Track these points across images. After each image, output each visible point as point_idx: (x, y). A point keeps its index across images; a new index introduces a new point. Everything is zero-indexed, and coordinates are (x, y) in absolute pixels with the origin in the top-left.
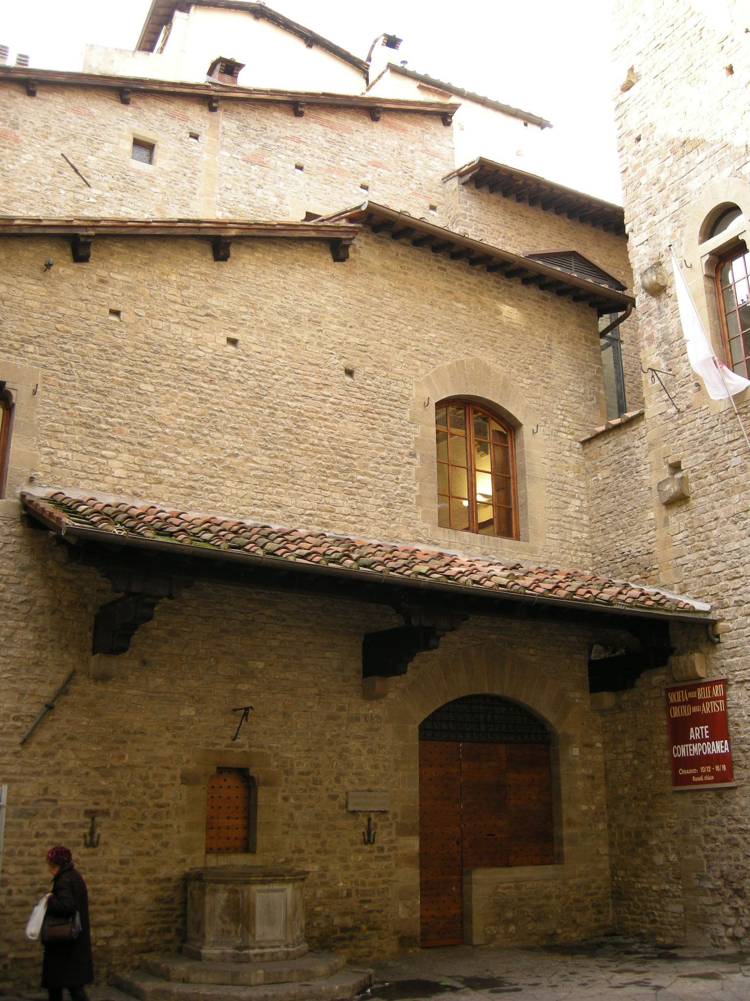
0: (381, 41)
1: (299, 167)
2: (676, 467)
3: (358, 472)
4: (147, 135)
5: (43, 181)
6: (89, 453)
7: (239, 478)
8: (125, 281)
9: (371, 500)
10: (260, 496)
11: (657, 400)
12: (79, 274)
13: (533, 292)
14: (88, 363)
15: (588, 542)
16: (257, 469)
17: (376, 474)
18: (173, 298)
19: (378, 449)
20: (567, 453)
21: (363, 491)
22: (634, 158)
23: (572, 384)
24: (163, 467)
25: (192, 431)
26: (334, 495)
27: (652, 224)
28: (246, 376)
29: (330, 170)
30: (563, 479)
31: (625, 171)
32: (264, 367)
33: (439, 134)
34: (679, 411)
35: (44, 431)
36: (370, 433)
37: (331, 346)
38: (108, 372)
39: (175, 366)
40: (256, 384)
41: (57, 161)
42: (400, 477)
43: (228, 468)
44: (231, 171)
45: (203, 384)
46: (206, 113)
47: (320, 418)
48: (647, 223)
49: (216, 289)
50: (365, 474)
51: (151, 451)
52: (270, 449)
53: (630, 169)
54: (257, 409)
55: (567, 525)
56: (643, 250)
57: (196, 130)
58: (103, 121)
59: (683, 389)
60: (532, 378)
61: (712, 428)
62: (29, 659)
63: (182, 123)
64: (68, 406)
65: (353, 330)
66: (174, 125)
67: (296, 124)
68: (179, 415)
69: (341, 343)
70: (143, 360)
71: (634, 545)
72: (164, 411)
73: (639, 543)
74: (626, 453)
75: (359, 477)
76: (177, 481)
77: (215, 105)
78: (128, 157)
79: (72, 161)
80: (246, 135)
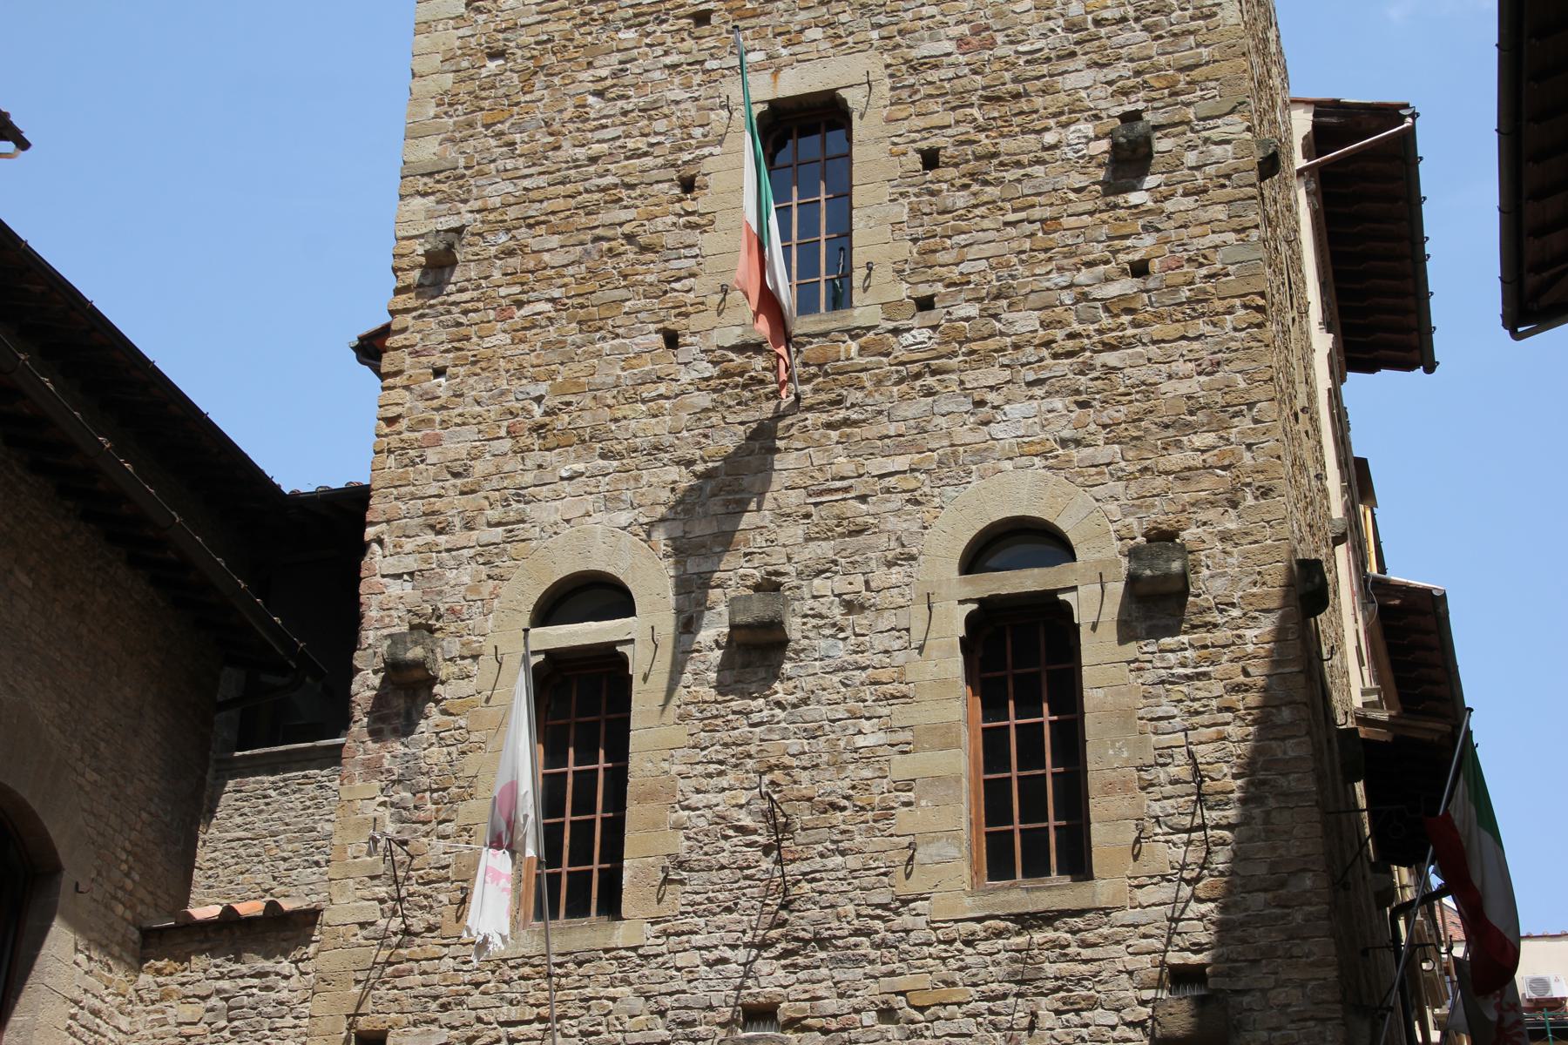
11: (359, 893)
22: (421, 405)
23: (156, 800)
27: (429, 547)
30: (98, 1004)
31: (390, 421)
48: (420, 541)
53: (403, 424)
56: (395, 588)
59: (425, 889)
60: (98, 770)
61: (477, 985)
74: (255, 981)
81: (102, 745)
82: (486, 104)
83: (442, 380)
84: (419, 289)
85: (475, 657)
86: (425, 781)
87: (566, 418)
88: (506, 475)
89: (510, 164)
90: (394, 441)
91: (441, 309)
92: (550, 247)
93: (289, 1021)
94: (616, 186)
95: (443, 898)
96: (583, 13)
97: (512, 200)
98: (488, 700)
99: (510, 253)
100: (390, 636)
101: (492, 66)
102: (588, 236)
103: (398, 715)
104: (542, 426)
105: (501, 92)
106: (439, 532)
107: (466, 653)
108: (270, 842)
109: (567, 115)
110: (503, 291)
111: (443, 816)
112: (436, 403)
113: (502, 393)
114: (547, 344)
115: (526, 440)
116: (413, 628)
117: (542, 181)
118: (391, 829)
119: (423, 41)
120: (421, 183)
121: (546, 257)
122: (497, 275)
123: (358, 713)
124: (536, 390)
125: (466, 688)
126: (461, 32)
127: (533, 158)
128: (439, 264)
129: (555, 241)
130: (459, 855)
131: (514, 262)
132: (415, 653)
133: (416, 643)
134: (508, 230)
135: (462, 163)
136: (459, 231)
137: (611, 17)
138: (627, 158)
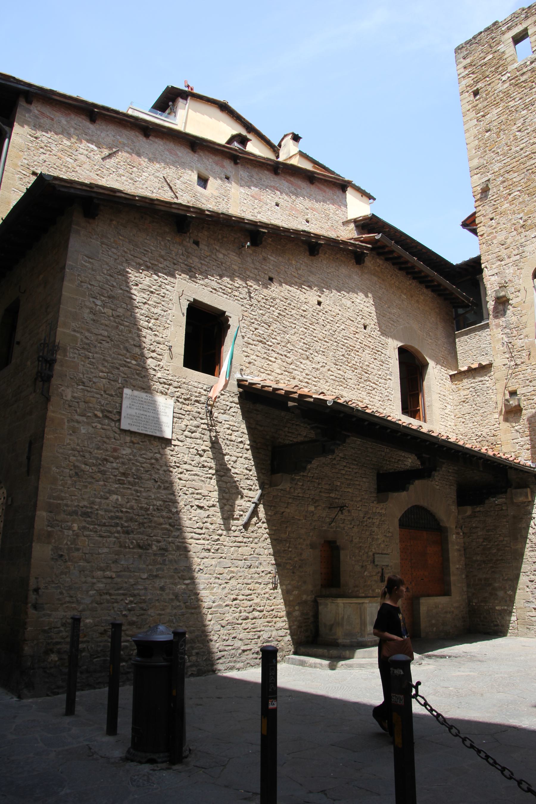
0: (290, 136)
1: (277, 205)
2: (513, 393)
3: (370, 381)
4: (205, 173)
5: (154, 191)
6: (264, 358)
7: (325, 379)
8: (274, 261)
9: (377, 397)
10: (334, 390)
12: (254, 254)
13: (429, 293)
14: (261, 306)
15: (454, 428)
16: (333, 375)
17: (378, 383)
18: (294, 274)
19: (378, 370)
20: (445, 380)
21: (373, 392)
22: (489, 229)
24: (295, 370)
25: (306, 351)
26: (363, 393)
27: (500, 265)
28: (326, 323)
29: (292, 209)
30: (444, 394)
32: (332, 319)
33: (340, 197)
34: (516, 365)
35: (244, 343)
36: (374, 361)
37: (358, 311)
38: (270, 313)
39: (298, 313)
40: (330, 327)
41: (161, 180)
42: (387, 386)
43: (321, 373)
44: (245, 201)
45: (309, 325)
46: (232, 164)
47: (355, 350)
48: (497, 264)
49: (311, 272)
50: (374, 383)
51: (290, 360)
52: (337, 365)
53: (485, 235)
54: (332, 342)
55: (447, 418)
56: (493, 278)
57: (229, 174)
58: (183, 160)
59: (519, 353)
62: (244, 475)
63: (221, 169)
64: (254, 330)
65: (365, 304)
66: (217, 169)
67: (275, 180)
68: (300, 341)
69: (362, 311)
70: (284, 307)
71: (485, 431)
72: (295, 338)
73: (488, 430)
74: (480, 383)
75: (372, 384)
76: (301, 378)
77: (238, 161)
78: (196, 184)
79: (168, 181)
80: (253, 182)
81: (430, 333)
82: (488, 145)
83: (493, 221)
84: (481, 199)
85: (519, 291)
86: (512, 326)
87: (530, 221)
88: (517, 241)
89: (498, 158)
90: (484, 241)
91: (488, 202)
92: (515, 177)
93: (491, 391)
94: (530, 154)
95: (524, 354)
96: (509, 111)
97: (501, 168)
98: (524, 302)
99: (504, 182)
100: (495, 291)
101: (487, 134)
102: (525, 170)
103: (501, 311)
104: (524, 225)
105: (491, 140)
106: (502, 261)
107: (516, 290)
108: (470, 352)
109: (511, 140)
110: (504, 193)
111: (519, 334)
112: (493, 227)
113: (510, 220)
114: (520, 203)
115: (520, 230)
116: (500, 287)
117: (508, 160)
118: (506, 340)
119: (467, 134)
120: (475, 172)
121: (514, 180)
122: (502, 189)
123: (491, 313)
124: (519, 216)
125: (518, 300)
126: (477, 129)
127: (504, 155)
128: (485, 191)
129: (516, 174)
130: (526, 343)
131: (505, 184)
132: (502, 294)
133: (502, 291)
134: (502, 176)
135: (485, 162)
136: (489, 180)
137: (518, 109)
138: (531, 145)
